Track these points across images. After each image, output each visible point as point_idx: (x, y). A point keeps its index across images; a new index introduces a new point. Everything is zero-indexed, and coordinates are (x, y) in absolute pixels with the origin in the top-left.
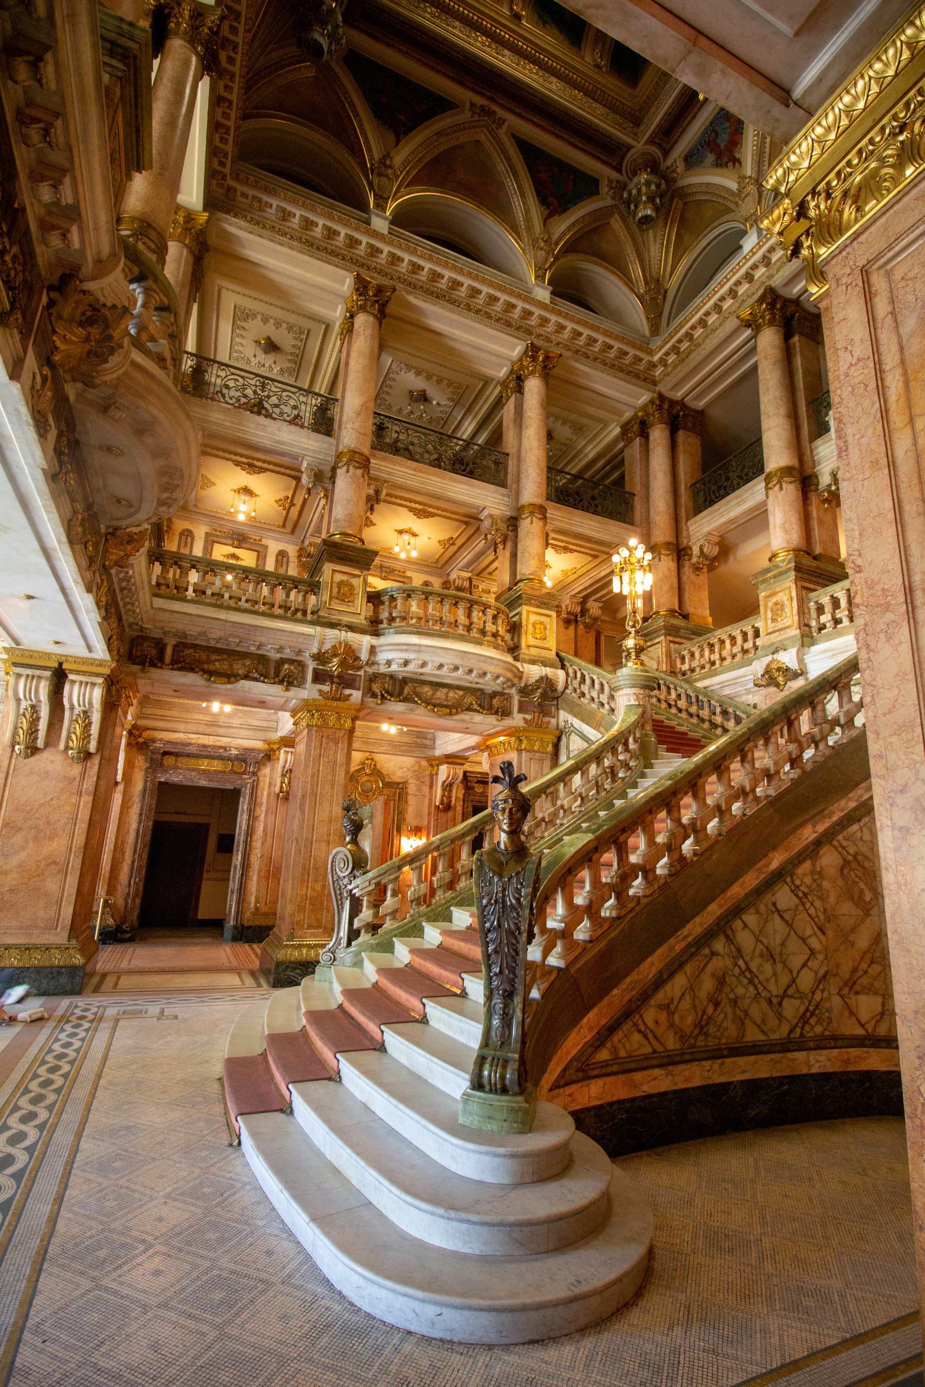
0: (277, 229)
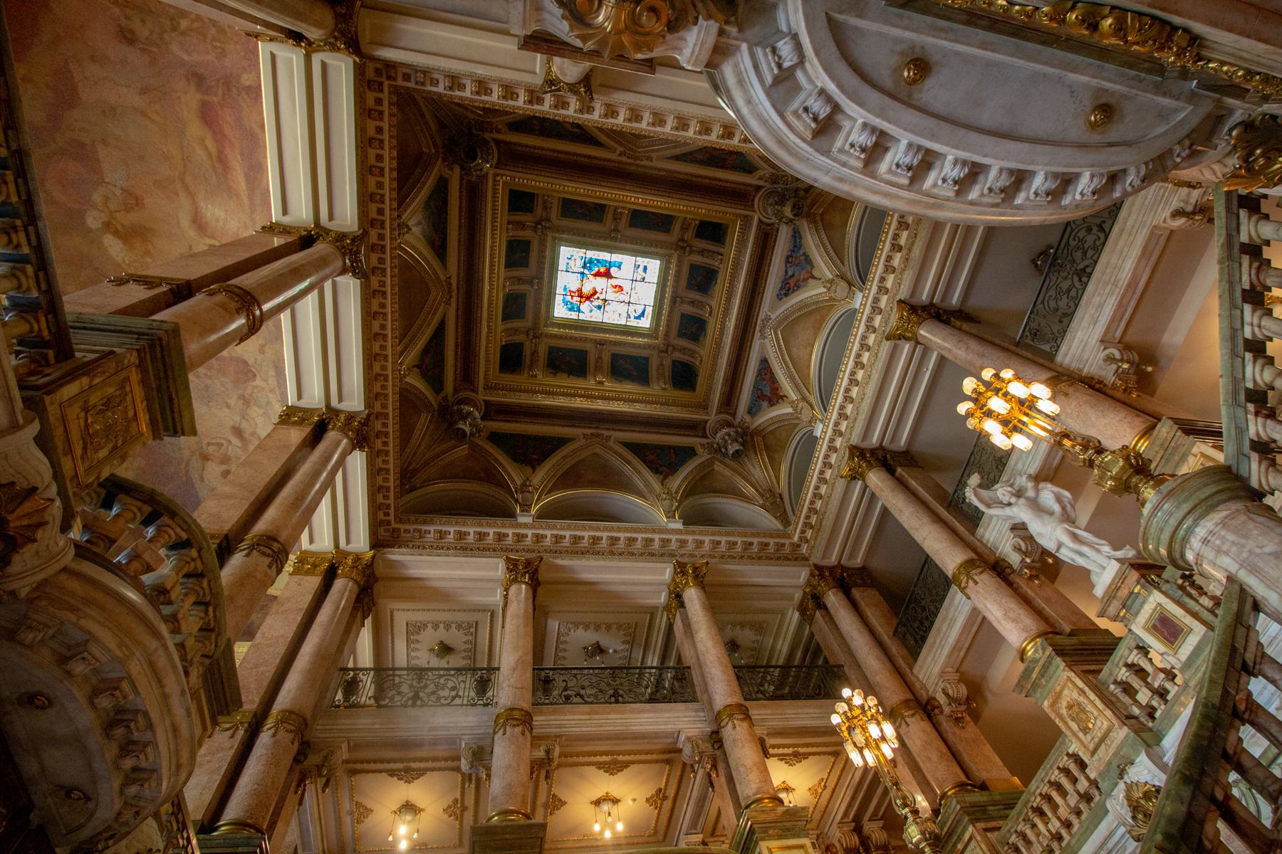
0: (440, 546)
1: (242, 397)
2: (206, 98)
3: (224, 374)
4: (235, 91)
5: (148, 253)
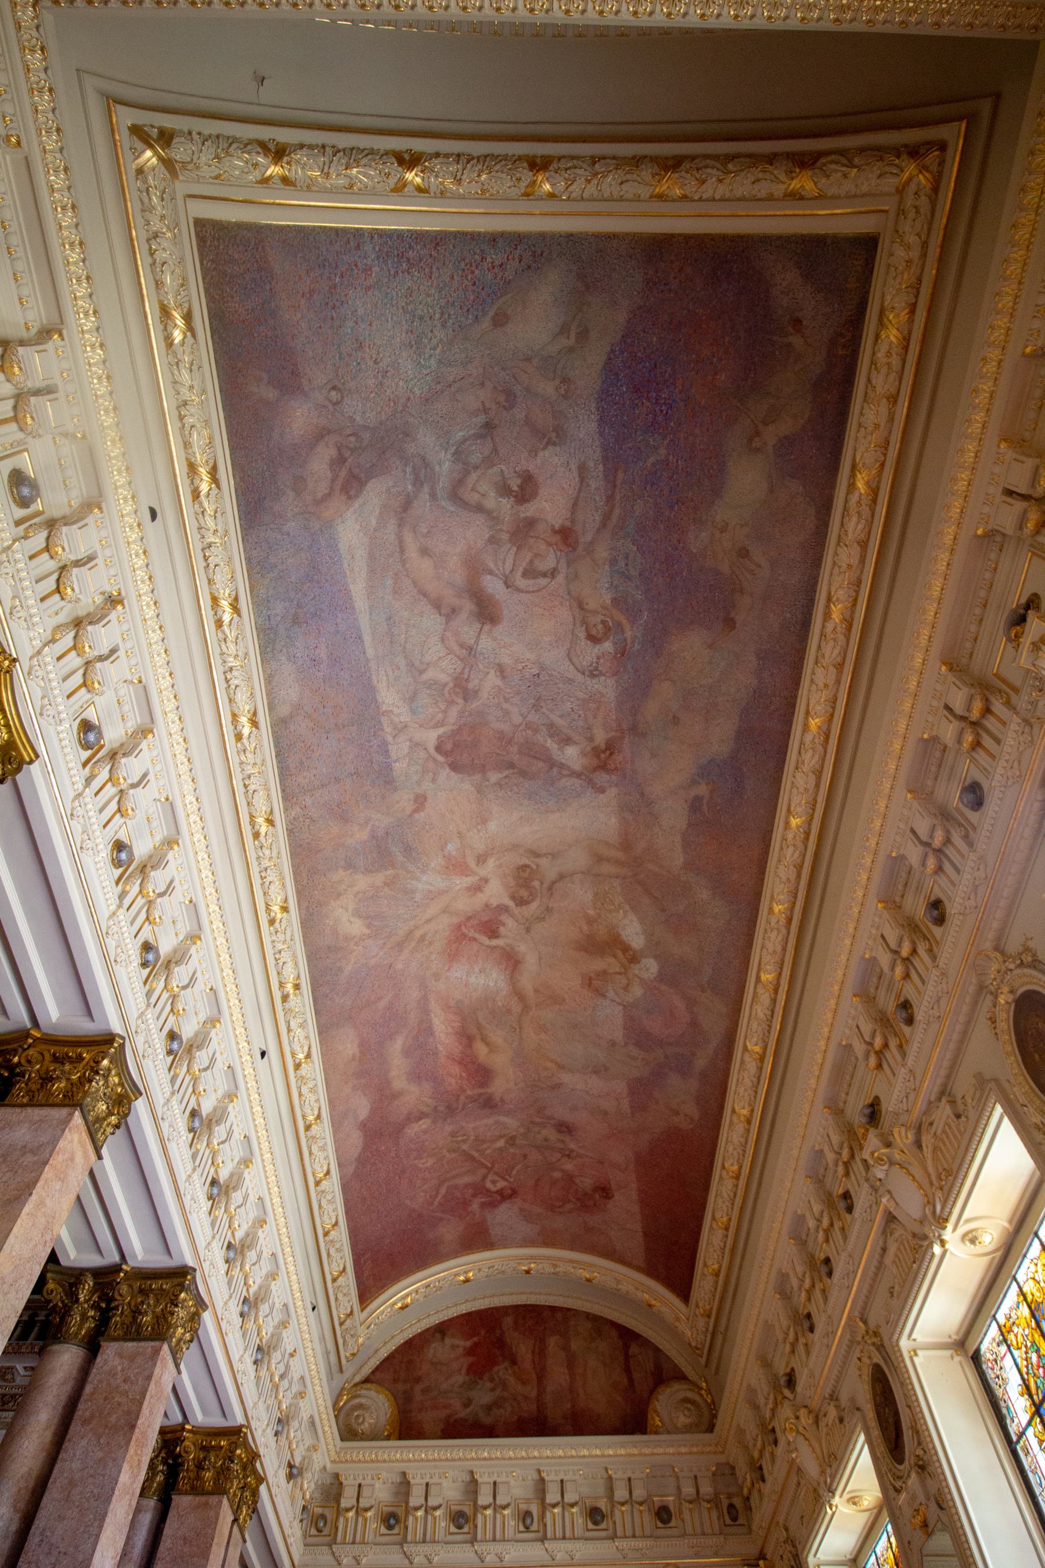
1: (468, 695)
2: (481, 1091)
3: (501, 735)
4: (441, 1108)
5: (590, 921)
